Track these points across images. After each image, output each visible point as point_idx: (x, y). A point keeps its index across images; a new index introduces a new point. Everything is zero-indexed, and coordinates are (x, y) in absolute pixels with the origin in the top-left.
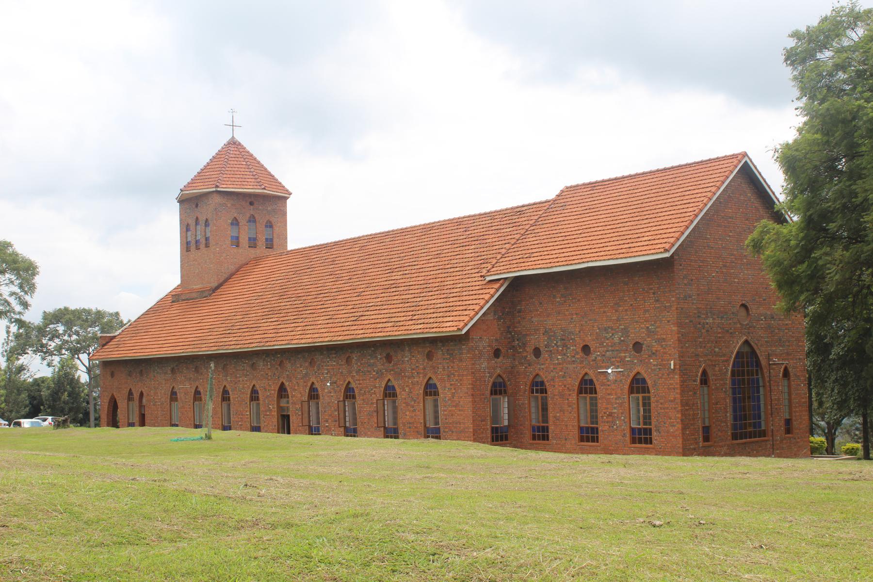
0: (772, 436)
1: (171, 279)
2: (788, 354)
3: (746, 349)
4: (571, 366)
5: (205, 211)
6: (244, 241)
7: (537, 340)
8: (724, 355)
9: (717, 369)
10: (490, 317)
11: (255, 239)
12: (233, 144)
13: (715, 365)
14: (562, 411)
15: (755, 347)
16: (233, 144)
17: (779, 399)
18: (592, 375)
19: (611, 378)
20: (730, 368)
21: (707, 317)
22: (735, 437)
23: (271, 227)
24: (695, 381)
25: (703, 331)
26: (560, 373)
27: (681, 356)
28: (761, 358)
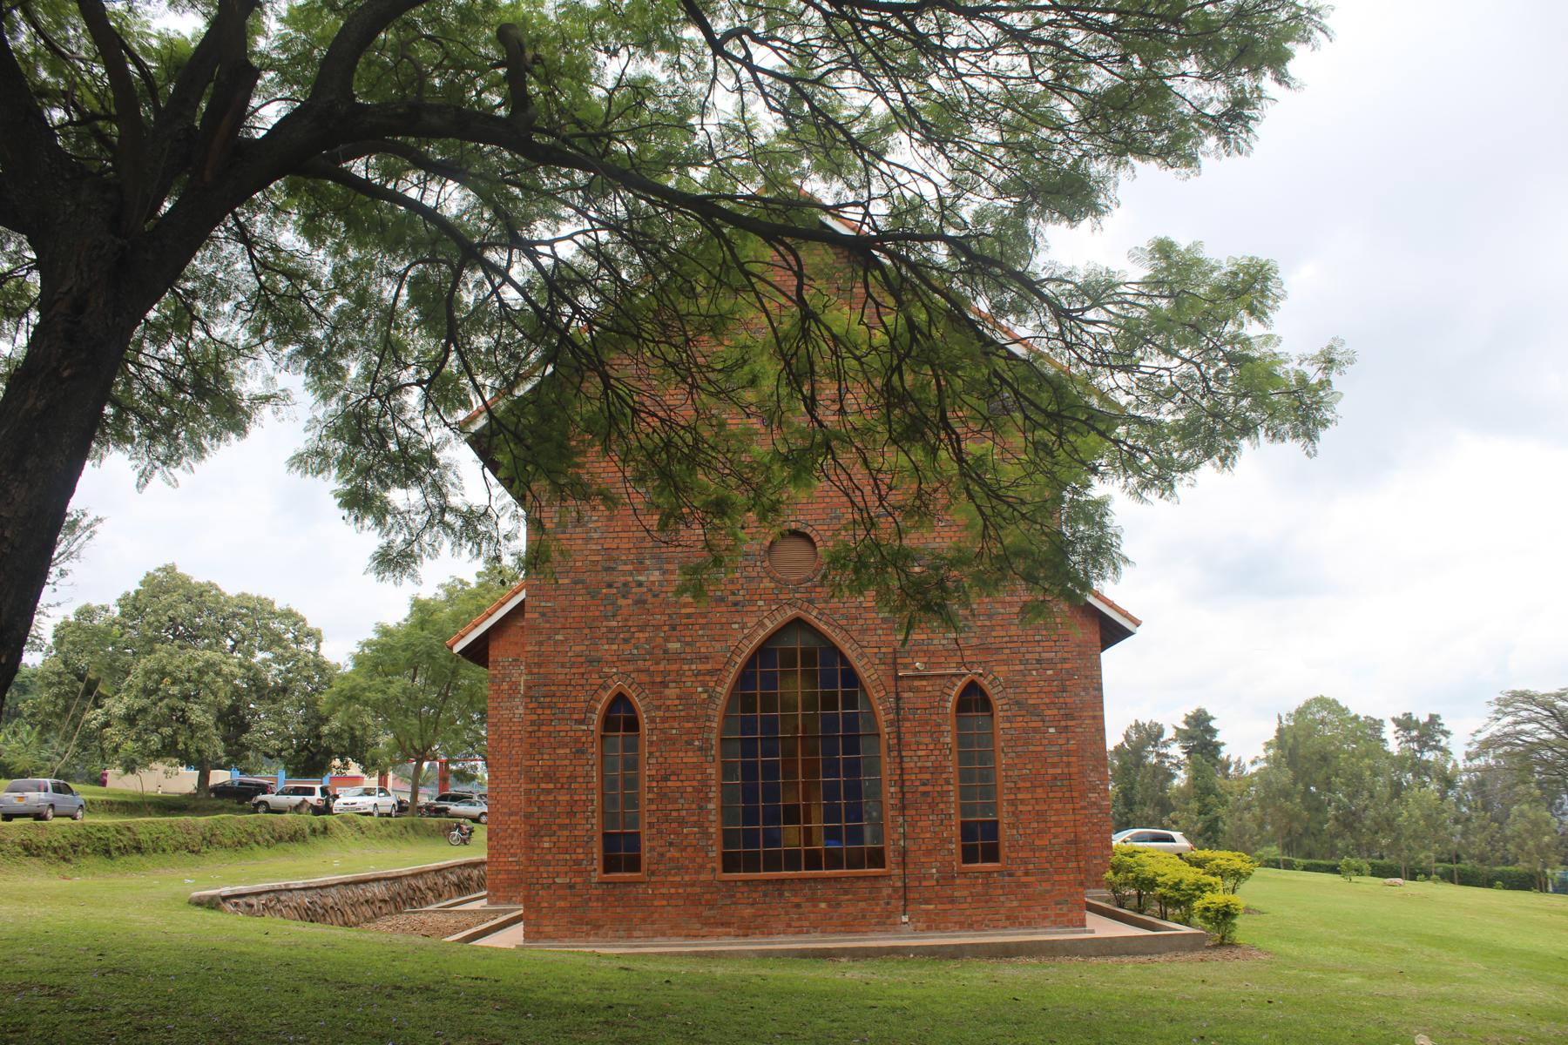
0: (903, 864)
3: (797, 642)
9: (672, 692)
13: (664, 685)
15: (837, 637)
17: (938, 769)
20: (723, 690)
21: (640, 566)
22: (730, 863)
25: (621, 602)
28: (858, 664)
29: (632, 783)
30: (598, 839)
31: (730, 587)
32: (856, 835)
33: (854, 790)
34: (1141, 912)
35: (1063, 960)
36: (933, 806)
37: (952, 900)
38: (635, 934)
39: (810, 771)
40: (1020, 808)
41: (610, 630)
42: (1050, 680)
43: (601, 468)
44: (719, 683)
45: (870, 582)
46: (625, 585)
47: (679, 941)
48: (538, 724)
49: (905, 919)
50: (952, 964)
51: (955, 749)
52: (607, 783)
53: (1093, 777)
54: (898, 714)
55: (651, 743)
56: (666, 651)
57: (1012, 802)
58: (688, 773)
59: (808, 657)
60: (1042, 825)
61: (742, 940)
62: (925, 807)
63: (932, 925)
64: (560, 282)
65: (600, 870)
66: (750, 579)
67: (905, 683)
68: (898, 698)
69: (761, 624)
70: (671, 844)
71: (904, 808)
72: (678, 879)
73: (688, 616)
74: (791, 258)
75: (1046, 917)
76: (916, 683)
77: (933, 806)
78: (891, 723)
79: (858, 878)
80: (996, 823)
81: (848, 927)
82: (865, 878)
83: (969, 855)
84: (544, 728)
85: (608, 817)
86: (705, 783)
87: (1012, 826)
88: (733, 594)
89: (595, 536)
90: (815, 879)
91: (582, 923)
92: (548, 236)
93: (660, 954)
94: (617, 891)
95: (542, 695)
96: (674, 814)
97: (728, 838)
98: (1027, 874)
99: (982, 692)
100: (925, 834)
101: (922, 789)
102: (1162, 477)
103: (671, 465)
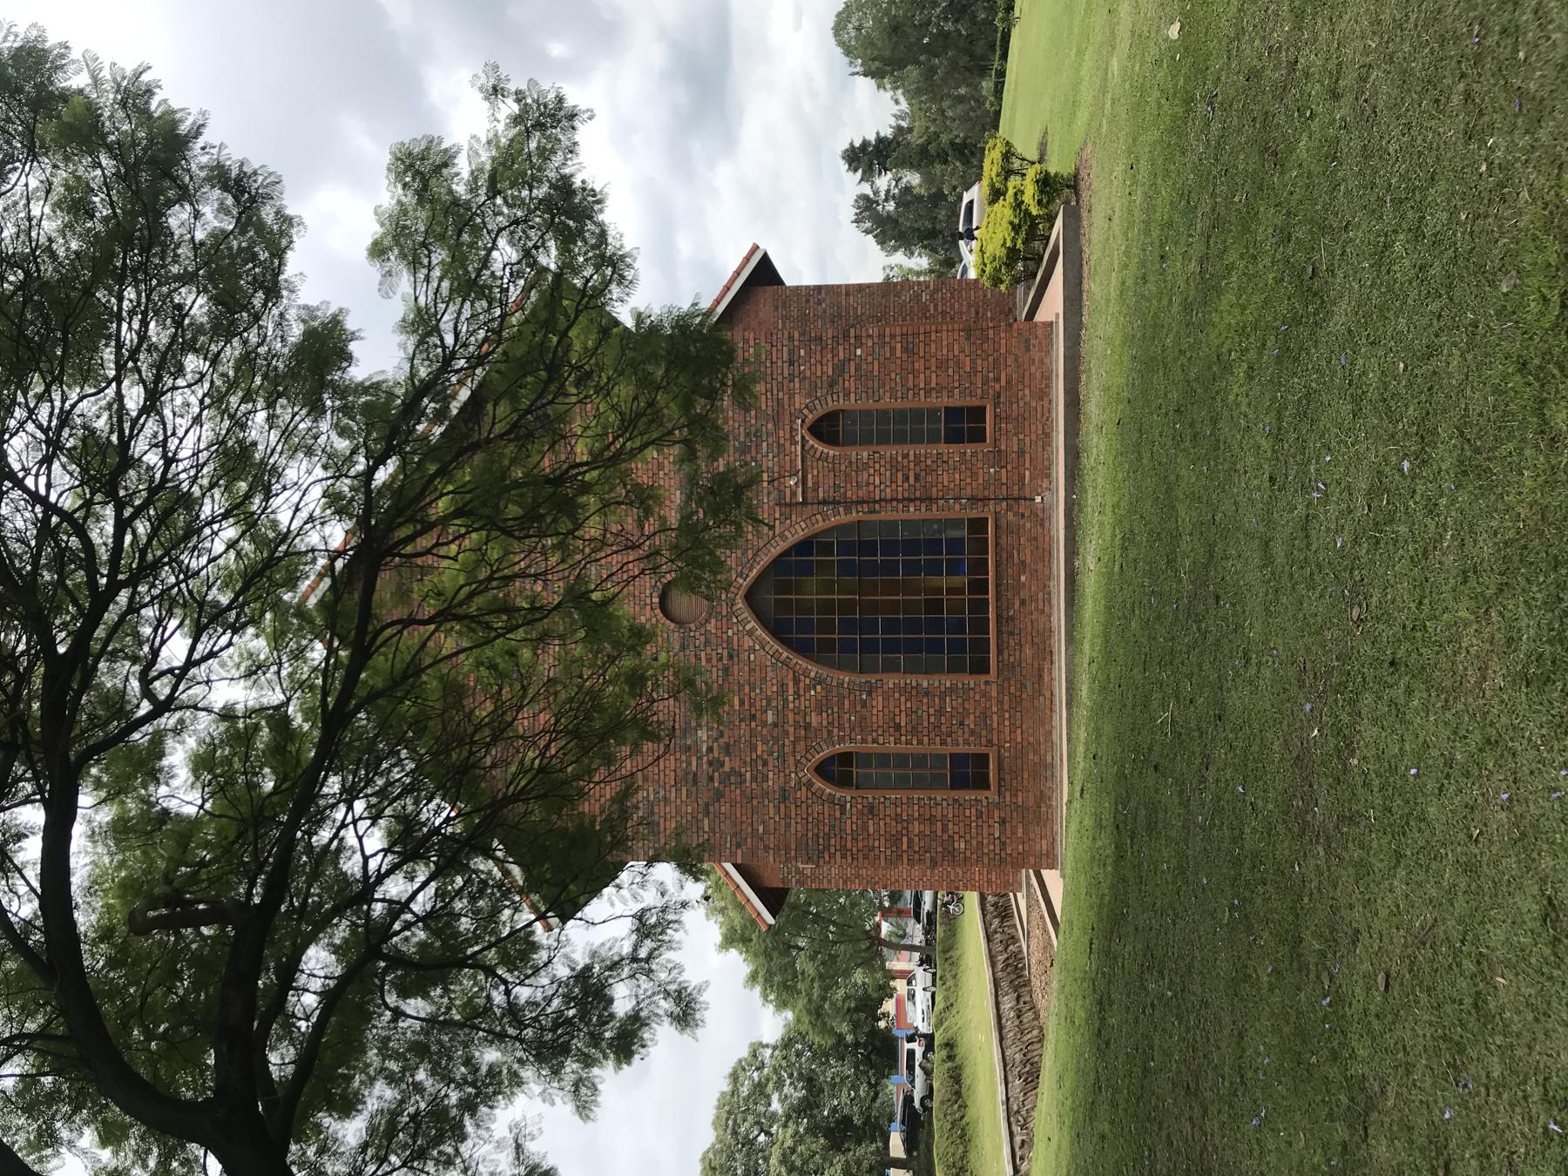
0: (985, 499)
3: (769, 597)
8: (783, 687)
9: (814, 720)
13: (807, 727)
15: (765, 560)
22: (981, 667)
24: (843, 807)
25: (727, 768)
28: (791, 540)
29: (902, 760)
30: (956, 794)
31: (714, 661)
32: (955, 545)
33: (912, 546)
34: (1041, 258)
35: (1085, 348)
36: (929, 471)
37: (1021, 453)
38: (1049, 759)
39: (893, 588)
40: (933, 385)
41: (754, 779)
42: (809, 353)
43: (597, 799)
44: (806, 674)
45: (712, 553)
46: (710, 763)
47: (1056, 718)
48: (844, 851)
49: (1038, 499)
50: (1084, 460)
51: (875, 448)
52: (902, 783)
53: (906, 297)
54: (839, 503)
55: (864, 741)
56: (775, 725)
57: (928, 393)
58: (893, 706)
59: (783, 588)
60: (951, 363)
61: (1056, 657)
62: (929, 479)
63: (1046, 473)
64: (409, 844)
65: (987, 793)
66: (707, 642)
67: (810, 495)
68: (825, 502)
69: (750, 633)
70: (962, 724)
71: (930, 499)
72: (995, 717)
73: (742, 703)
74: (389, 632)
75: (1042, 361)
76: (810, 484)
77: (929, 471)
78: (848, 511)
79: (997, 544)
80: (947, 408)
81: (1045, 555)
82: (997, 537)
83: (978, 436)
84: (849, 845)
85: (934, 783)
86: (903, 690)
87: (951, 395)
88: (721, 659)
89: (662, 793)
90: (998, 585)
91: (1038, 813)
92: (358, 857)
93: (1069, 740)
94: (1008, 777)
95: (816, 850)
96: (932, 719)
97: (956, 668)
98: (997, 380)
99: (820, 420)
100: (953, 479)
101: (912, 481)
102: (613, 265)
103: (596, 728)
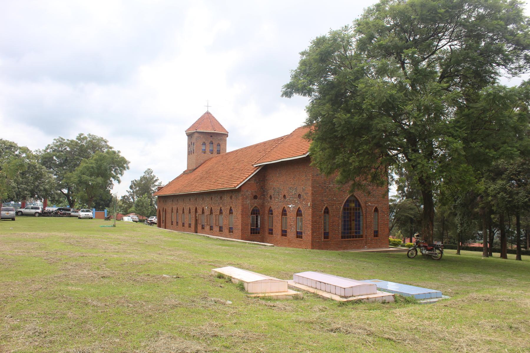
1: (183, 167)
2: (378, 201)
4: (280, 204)
5: (194, 140)
6: (208, 151)
7: (271, 192)
8: (339, 201)
9: (334, 207)
10: (253, 182)
11: (212, 150)
12: (208, 113)
14: (277, 223)
15: (358, 198)
16: (208, 113)
17: (371, 222)
18: (286, 208)
19: (291, 209)
20: (342, 207)
22: (342, 237)
23: (220, 145)
26: (276, 206)
27: (313, 201)
28: (361, 203)
32: (359, 233)
63: (369, 248)
85: (325, 230)
